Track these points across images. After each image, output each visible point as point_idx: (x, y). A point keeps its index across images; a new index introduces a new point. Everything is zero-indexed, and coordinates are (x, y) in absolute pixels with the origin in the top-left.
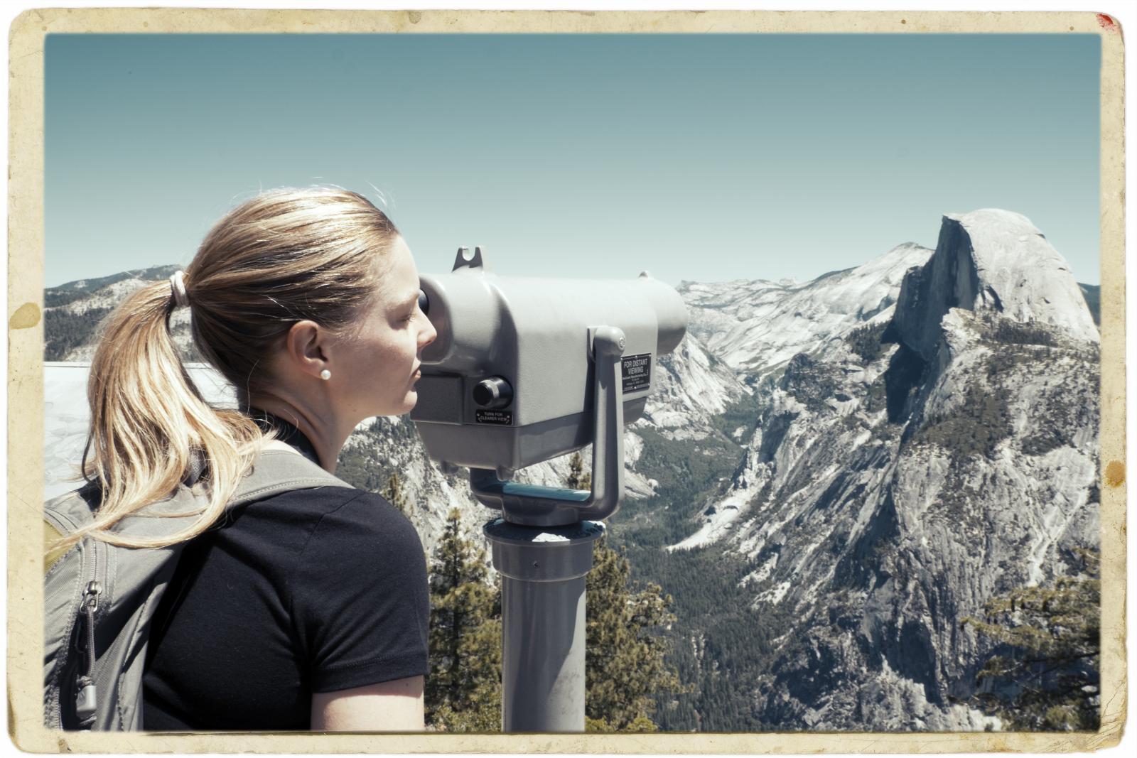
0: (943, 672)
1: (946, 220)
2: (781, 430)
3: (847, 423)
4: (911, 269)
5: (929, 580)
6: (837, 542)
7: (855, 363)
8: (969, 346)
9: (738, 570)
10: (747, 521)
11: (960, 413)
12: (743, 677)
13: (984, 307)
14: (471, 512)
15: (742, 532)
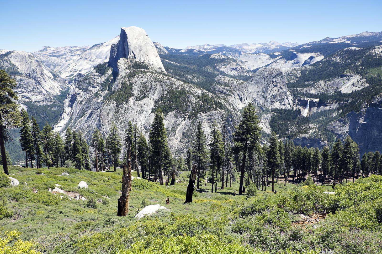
1: (122, 29)
3: (95, 95)
4: (113, 45)
7: (97, 76)
10: (65, 130)
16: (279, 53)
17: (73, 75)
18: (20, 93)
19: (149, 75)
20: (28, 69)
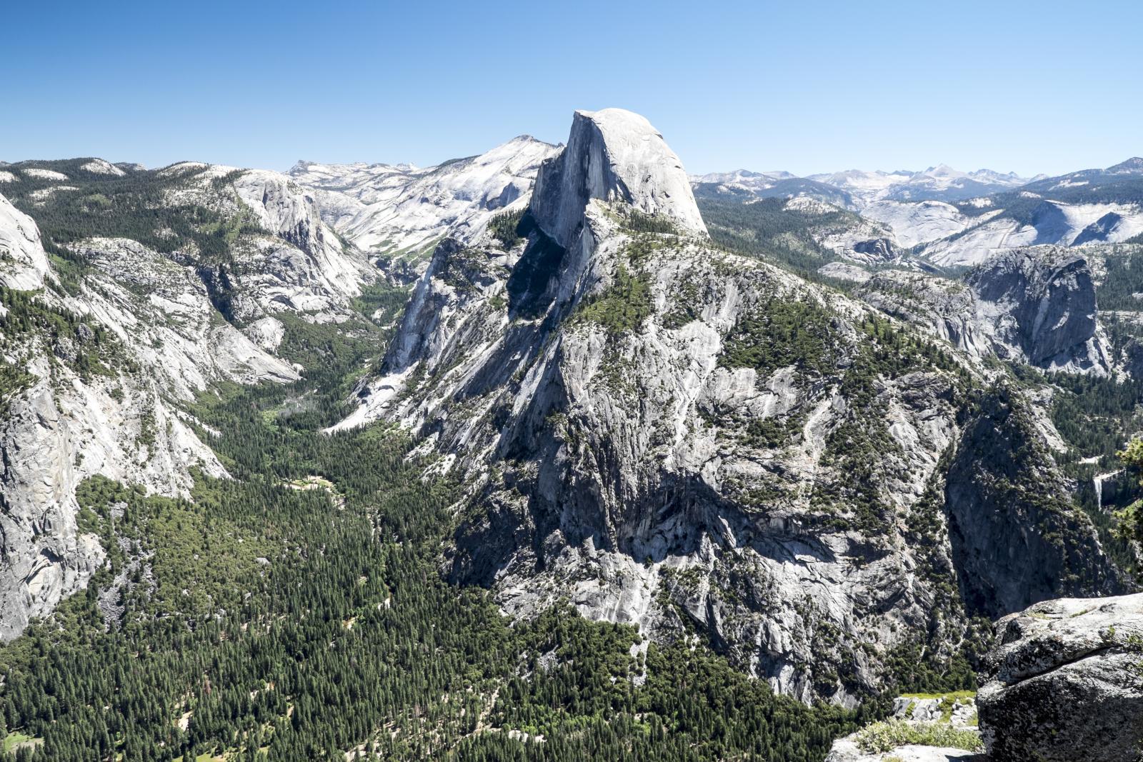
0: (611, 519)
1: (577, 117)
5: (597, 441)
6: (500, 417)
7: (497, 248)
8: (611, 234)
9: (403, 446)
10: (404, 399)
11: (610, 295)
12: (425, 546)
13: (616, 199)
14: (115, 410)
15: (402, 410)
16: (988, 203)
17: (390, 242)
19: (697, 253)
20: (285, 221)
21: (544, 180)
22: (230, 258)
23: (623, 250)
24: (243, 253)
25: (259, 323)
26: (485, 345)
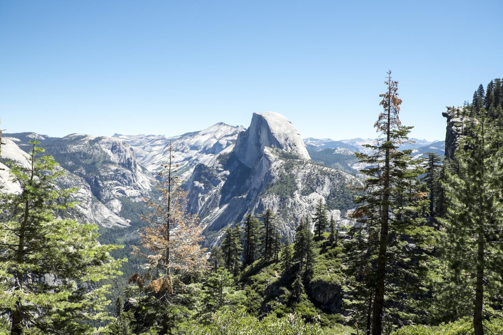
1: (254, 115)
2: (193, 194)
7: (221, 168)
8: (276, 160)
16: (417, 151)
18: (114, 186)
19: (312, 167)
21: (240, 140)
22: (99, 174)
23: (282, 166)
24: (104, 172)
25: (112, 202)
26: (218, 208)
